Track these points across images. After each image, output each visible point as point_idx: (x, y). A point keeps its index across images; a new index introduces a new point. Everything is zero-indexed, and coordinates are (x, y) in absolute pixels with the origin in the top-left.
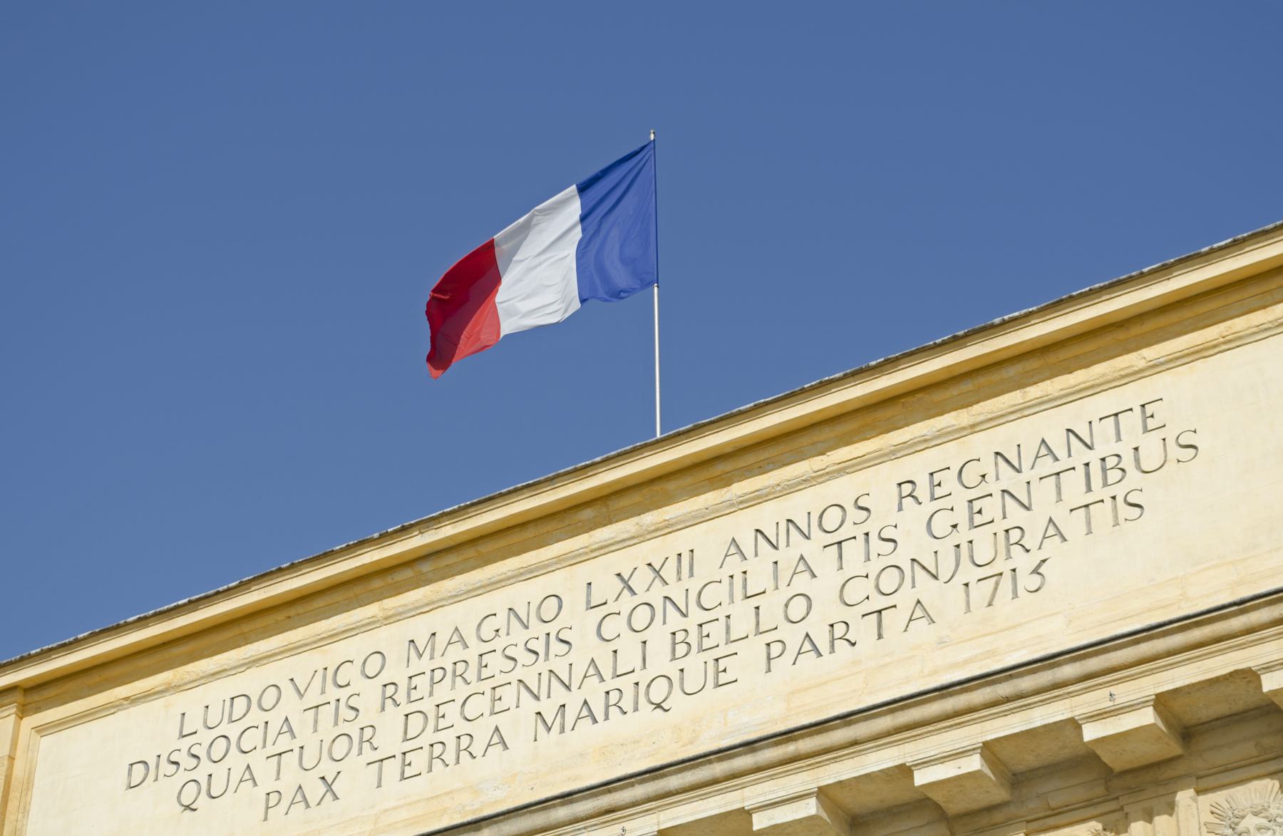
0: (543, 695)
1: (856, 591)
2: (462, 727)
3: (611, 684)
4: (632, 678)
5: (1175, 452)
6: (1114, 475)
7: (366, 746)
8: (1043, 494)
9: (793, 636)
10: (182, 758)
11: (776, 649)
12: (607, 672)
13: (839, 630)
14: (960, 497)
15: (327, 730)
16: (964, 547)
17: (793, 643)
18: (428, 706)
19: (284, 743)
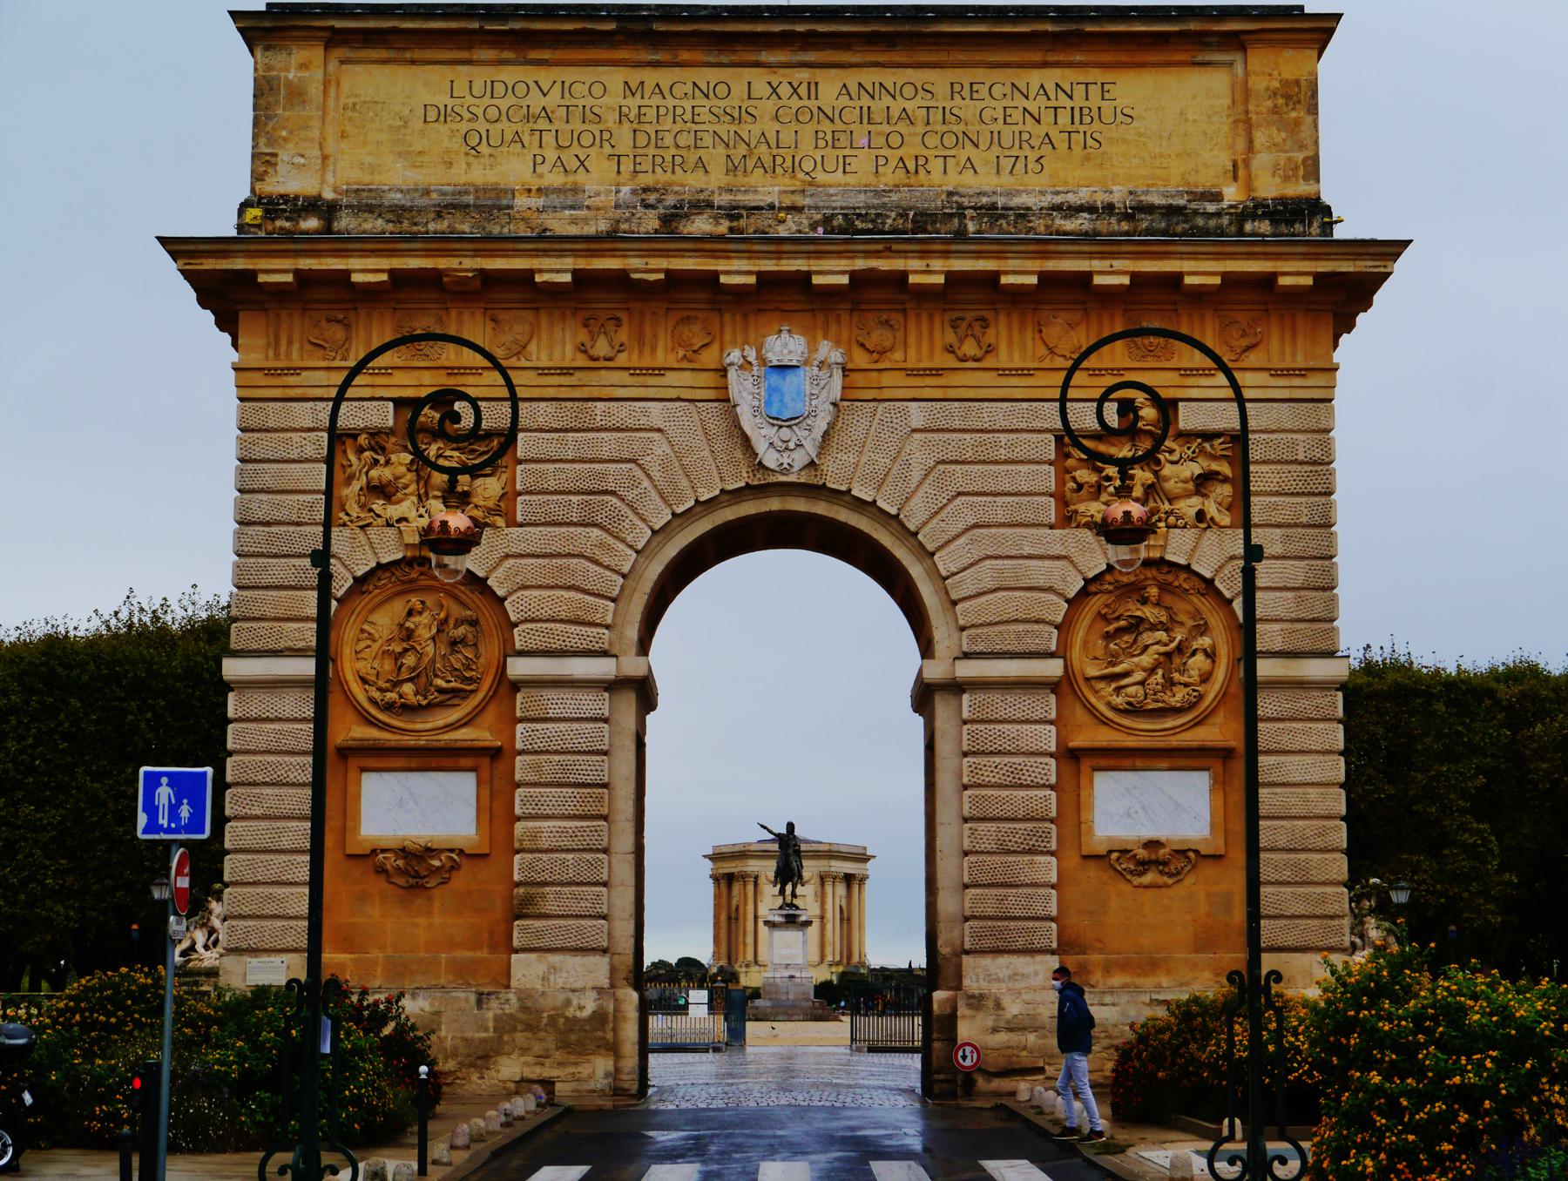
0: (732, 143)
1: (932, 141)
2: (673, 151)
3: (775, 152)
4: (791, 151)
5: (1120, 117)
6: (1087, 119)
7: (606, 144)
8: (1048, 117)
9: (893, 156)
10: (467, 115)
11: (881, 161)
12: (773, 143)
13: (921, 161)
14: (999, 105)
15: (577, 126)
16: (996, 134)
17: (893, 162)
18: (651, 129)
19: (542, 124)
